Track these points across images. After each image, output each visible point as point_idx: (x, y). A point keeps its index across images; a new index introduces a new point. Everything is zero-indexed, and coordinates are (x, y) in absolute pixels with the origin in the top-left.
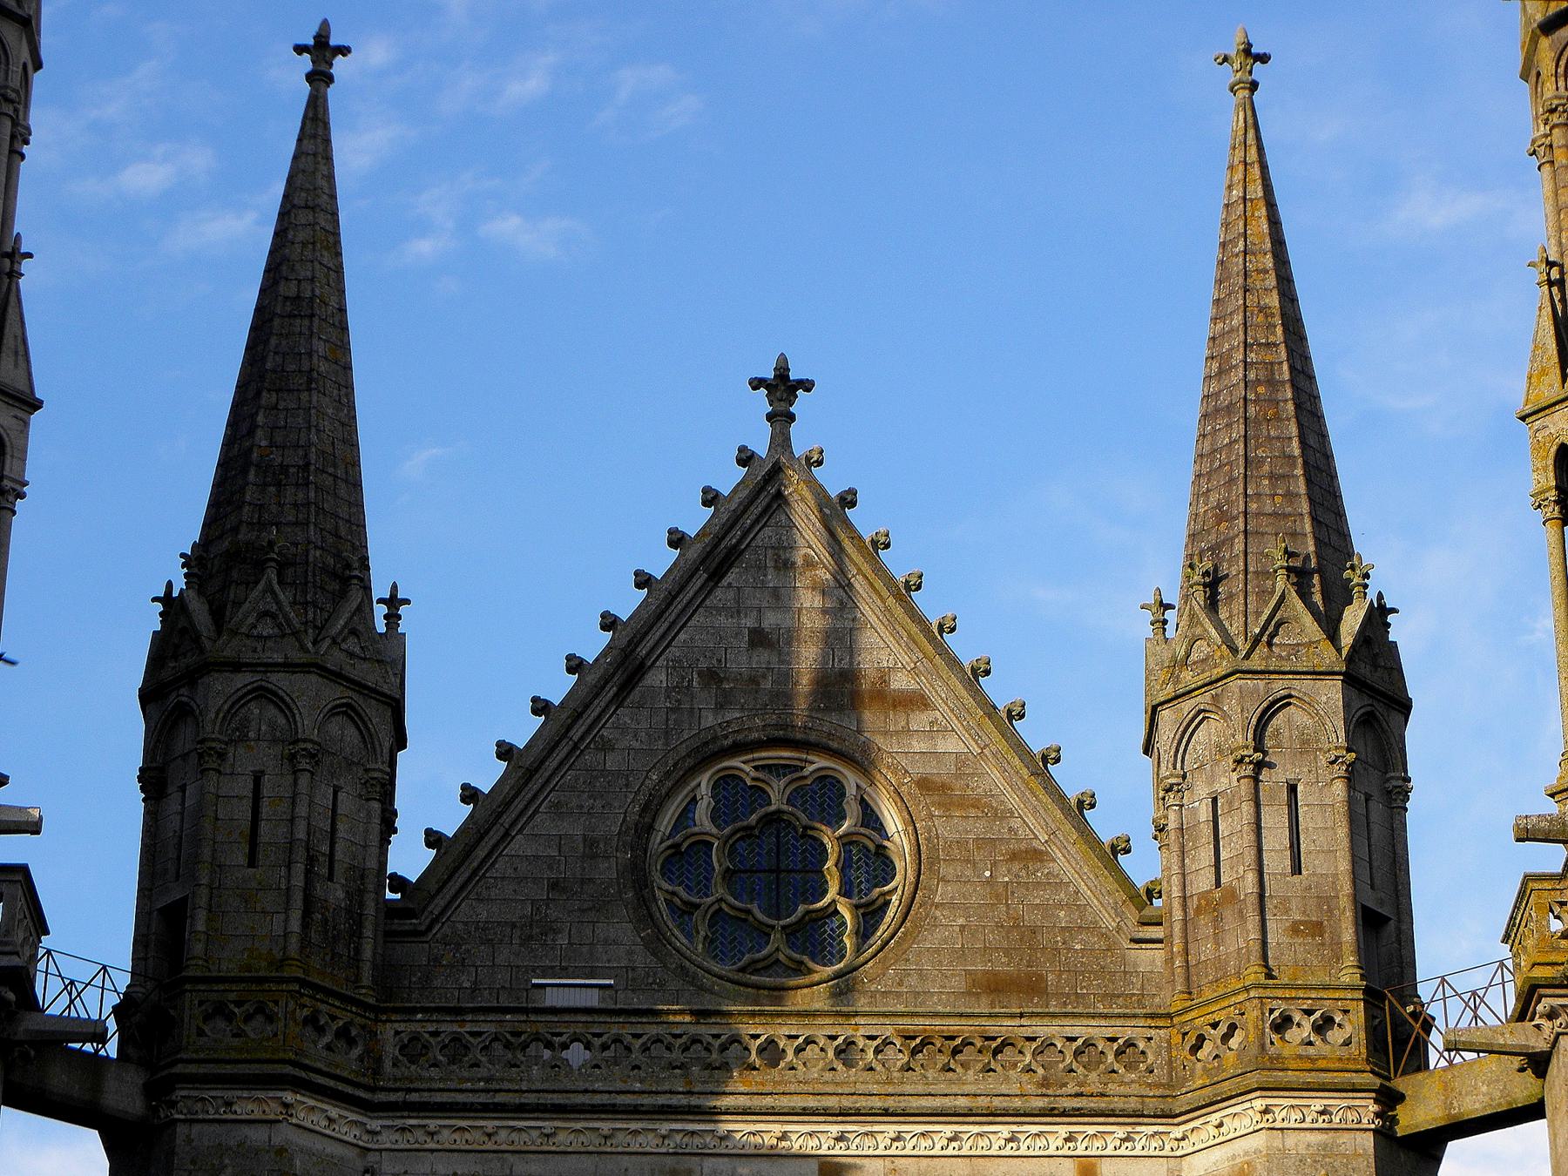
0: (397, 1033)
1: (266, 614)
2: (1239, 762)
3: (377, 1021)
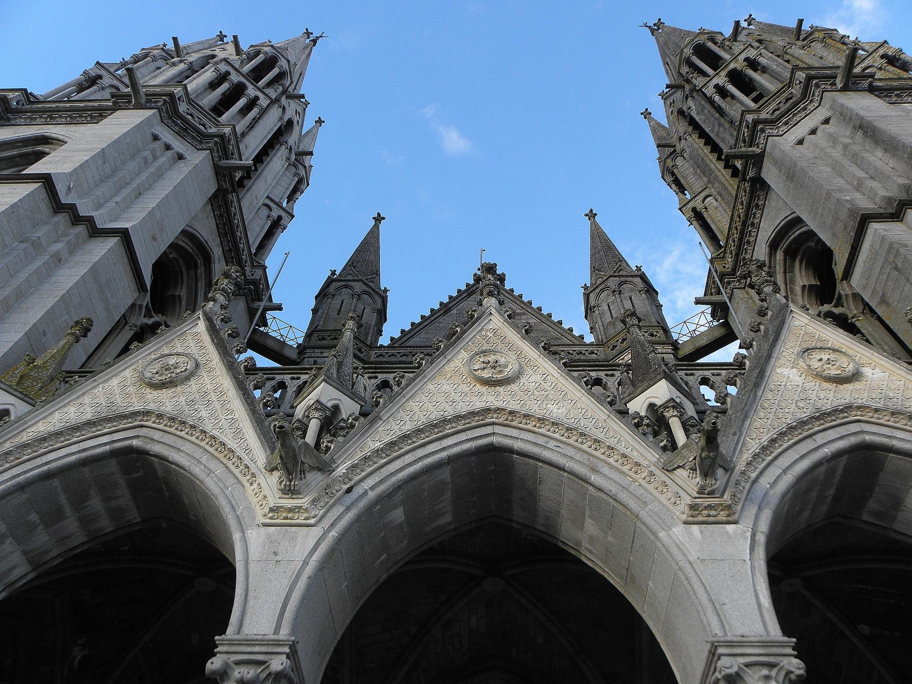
0: (376, 353)
1: (350, 274)
2: (614, 291)
3: (370, 350)
